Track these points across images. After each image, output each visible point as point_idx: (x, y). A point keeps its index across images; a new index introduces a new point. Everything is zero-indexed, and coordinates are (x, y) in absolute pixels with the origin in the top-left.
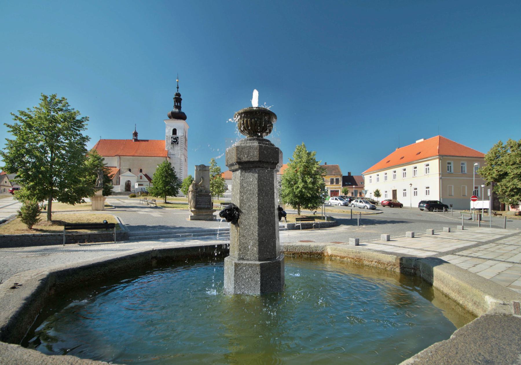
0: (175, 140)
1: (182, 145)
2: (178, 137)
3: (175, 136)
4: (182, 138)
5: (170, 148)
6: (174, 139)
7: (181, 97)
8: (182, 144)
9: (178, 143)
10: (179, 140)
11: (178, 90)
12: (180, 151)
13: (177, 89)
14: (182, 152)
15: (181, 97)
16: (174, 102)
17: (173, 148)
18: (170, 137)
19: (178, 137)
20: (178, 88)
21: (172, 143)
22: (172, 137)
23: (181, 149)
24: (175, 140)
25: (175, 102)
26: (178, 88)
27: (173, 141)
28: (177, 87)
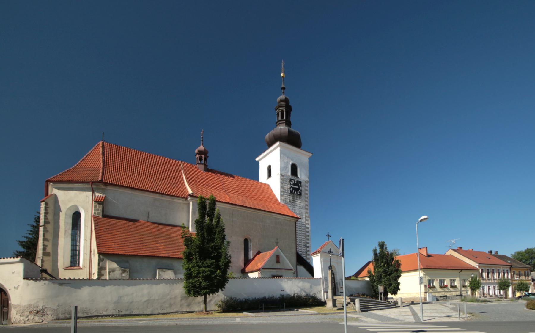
0: (298, 187)
1: (306, 199)
4: (306, 184)
5: (288, 200)
6: (294, 184)
8: (307, 198)
9: (300, 194)
10: (302, 189)
12: (304, 211)
14: (307, 213)
17: (293, 202)
18: (287, 179)
19: (300, 182)
21: (291, 192)
22: (291, 180)
23: (307, 207)
24: (298, 187)
27: (294, 188)
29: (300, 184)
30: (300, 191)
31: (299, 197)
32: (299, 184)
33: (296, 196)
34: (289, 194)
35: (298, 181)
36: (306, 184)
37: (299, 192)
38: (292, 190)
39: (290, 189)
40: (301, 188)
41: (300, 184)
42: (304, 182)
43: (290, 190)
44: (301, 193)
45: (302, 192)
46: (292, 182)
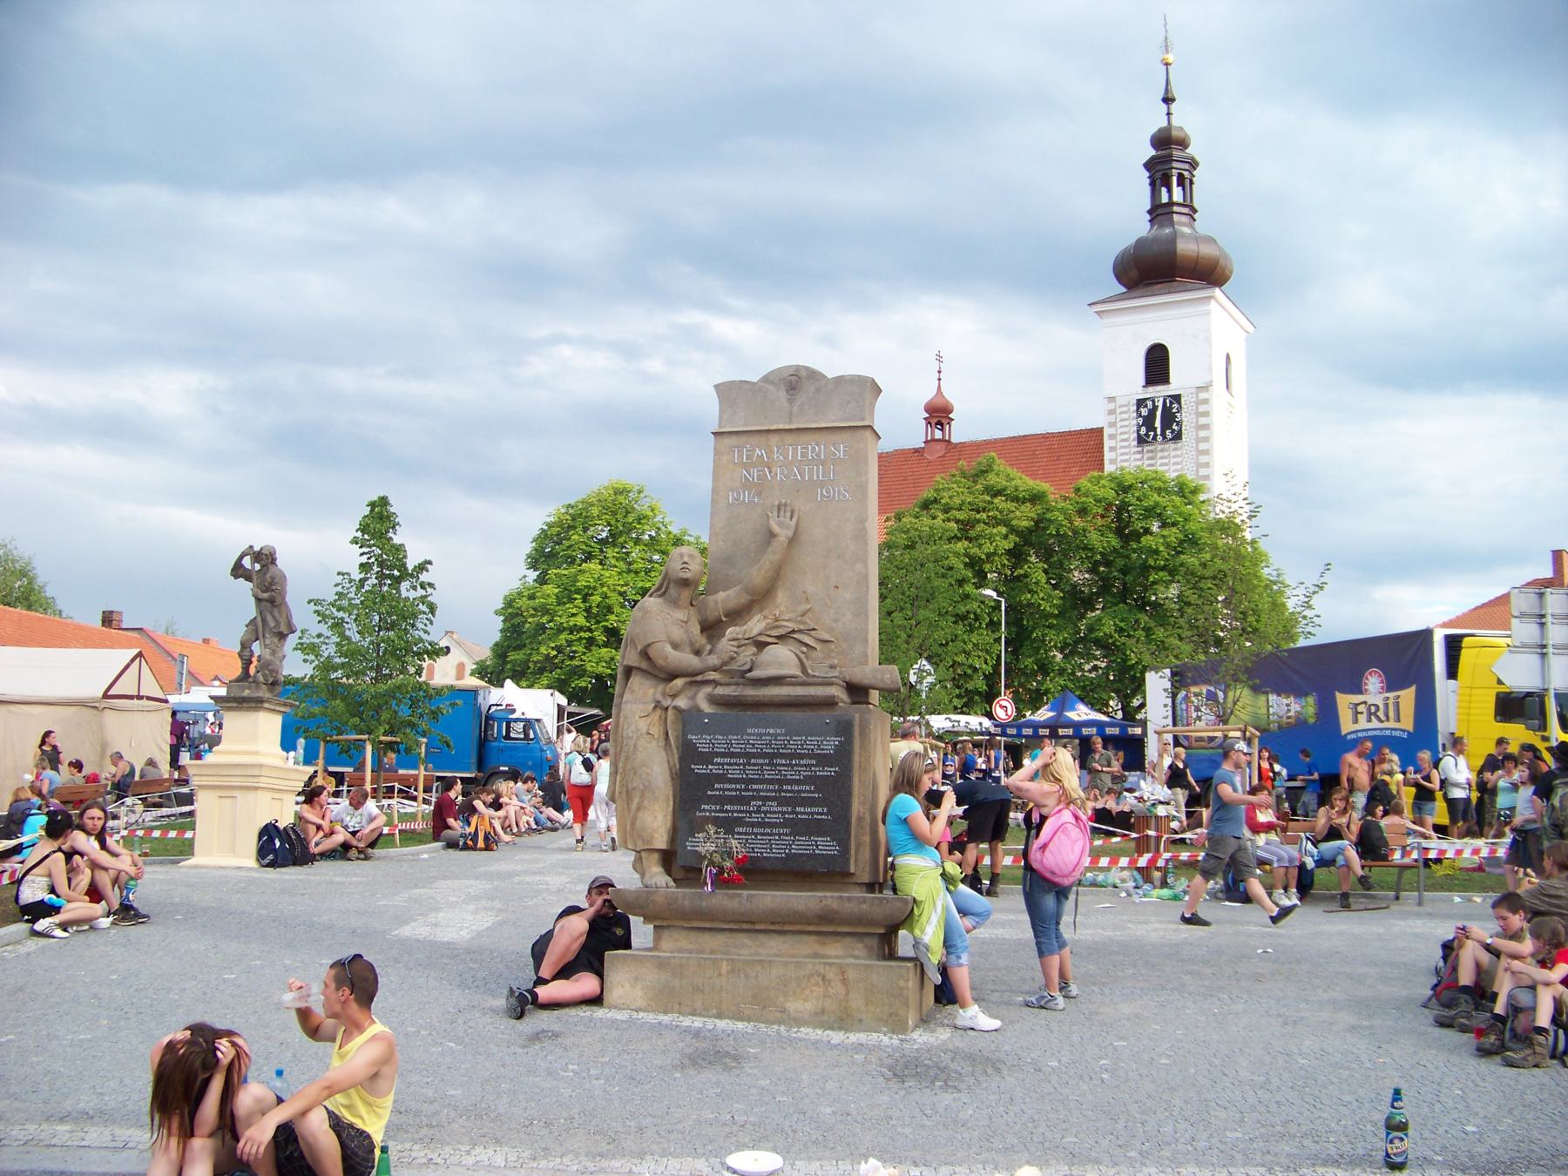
2: (1177, 398)
3: (1159, 392)
4: (1203, 396)
7: (1153, 152)
9: (1178, 436)
11: (1169, 114)
13: (1164, 106)
15: (1153, 152)
16: (1148, 189)
19: (1177, 398)
20: (1168, 100)
22: (1140, 403)
25: (1152, 184)
26: (1168, 100)
28: (1161, 94)
29: (1176, 405)
30: (1175, 427)
31: (1171, 445)
32: (1171, 403)
33: (1160, 447)
34: (1136, 449)
35: (1169, 396)
36: (1203, 396)
37: (1173, 431)
38: (1147, 435)
39: (1138, 431)
40: (1178, 415)
41: (1176, 405)
42: (1194, 390)
43: (1139, 435)
44: (1181, 430)
45: (1183, 428)
46: (1146, 406)
